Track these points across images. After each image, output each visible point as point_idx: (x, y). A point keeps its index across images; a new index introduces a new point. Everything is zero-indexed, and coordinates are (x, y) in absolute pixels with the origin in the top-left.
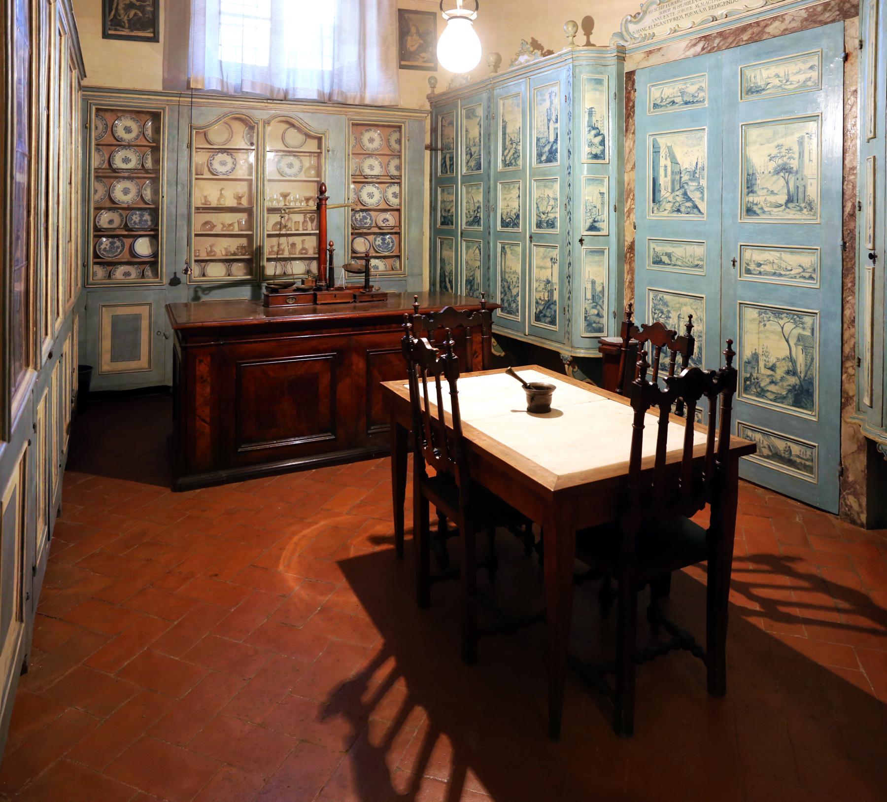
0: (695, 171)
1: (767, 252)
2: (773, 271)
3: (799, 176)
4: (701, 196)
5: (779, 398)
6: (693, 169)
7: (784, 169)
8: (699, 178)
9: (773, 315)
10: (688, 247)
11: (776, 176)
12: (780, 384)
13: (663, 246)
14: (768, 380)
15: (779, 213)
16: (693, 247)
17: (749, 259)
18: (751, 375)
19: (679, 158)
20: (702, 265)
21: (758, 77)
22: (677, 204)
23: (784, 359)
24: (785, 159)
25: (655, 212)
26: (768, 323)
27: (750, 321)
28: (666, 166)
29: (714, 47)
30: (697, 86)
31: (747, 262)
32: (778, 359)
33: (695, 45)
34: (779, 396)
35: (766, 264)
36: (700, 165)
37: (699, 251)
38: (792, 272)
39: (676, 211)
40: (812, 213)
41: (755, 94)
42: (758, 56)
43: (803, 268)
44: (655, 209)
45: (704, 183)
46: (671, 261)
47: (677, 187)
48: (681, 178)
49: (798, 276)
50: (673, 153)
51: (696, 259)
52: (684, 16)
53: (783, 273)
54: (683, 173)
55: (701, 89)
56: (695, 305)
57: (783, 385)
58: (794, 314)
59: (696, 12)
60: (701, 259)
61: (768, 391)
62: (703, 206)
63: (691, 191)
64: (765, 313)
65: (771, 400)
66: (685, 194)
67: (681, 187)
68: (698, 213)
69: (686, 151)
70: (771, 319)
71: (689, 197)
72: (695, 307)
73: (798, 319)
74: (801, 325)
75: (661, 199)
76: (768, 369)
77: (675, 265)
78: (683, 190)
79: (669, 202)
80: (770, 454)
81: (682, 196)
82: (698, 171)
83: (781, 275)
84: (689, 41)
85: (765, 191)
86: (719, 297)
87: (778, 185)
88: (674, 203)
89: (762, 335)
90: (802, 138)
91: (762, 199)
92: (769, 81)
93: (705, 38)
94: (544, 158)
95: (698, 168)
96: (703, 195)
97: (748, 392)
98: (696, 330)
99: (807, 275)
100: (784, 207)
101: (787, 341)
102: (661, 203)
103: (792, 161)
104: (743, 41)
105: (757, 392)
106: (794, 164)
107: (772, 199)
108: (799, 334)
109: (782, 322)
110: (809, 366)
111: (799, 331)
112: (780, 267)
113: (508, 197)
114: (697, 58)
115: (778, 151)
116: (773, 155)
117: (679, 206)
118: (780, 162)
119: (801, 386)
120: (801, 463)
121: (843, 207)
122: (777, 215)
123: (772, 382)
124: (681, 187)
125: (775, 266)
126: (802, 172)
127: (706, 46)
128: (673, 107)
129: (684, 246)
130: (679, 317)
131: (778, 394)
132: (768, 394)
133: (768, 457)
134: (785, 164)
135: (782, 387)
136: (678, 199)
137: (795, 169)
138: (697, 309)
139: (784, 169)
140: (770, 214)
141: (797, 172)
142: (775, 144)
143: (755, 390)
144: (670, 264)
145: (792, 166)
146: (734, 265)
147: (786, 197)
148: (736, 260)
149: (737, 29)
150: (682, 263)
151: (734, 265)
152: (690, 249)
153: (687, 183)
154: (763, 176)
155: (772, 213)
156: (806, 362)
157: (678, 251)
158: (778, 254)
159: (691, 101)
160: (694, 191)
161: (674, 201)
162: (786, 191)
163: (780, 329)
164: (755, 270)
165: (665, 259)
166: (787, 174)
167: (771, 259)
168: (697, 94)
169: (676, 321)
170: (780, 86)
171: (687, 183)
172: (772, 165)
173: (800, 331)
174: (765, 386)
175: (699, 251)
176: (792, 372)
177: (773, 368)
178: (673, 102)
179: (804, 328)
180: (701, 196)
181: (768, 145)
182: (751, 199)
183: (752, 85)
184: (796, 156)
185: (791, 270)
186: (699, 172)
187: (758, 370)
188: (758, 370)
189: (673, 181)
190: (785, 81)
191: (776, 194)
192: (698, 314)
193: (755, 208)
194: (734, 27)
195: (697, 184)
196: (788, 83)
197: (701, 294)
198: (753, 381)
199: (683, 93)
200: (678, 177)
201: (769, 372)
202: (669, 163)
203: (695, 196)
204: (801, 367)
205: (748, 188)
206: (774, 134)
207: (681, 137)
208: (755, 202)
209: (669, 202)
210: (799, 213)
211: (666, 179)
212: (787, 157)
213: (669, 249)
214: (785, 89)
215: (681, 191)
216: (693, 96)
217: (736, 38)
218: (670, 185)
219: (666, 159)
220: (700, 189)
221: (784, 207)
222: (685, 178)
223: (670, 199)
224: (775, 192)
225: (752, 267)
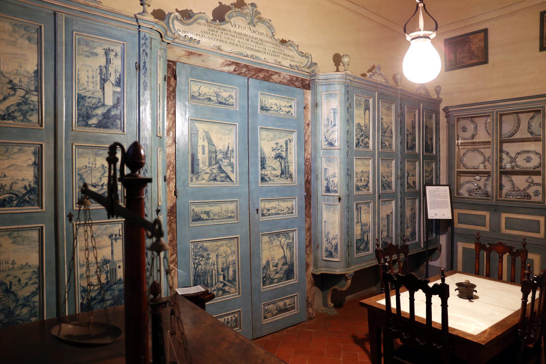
0: (227, 152)
1: (272, 202)
2: (276, 212)
3: (286, 161)
4: (232, 169)
5: (280, 280)
6: (226, 150)
7: (279, 156)
8: (230, 157)
9: (276, 236)
10: (223, 205)
12: (280, 272)
13: (202, 207)
14: (274, 273)
15: (278, 180)
16: (227, 204)
17: (263, 207)
18: (266, 274)
19: (214, 140)
20: (234, 216)
21: (267, 101)
22: (214, 175)
23: (281, 258)
24: (280, 151)
25: (194, 181)
26: (273, 242)
27: (265, 243)
28: (203, 146)
29: (242, 73)
30: (228, 94)
31: (262, 209)
32: (279, 259)
33: (229, 65)
34: (280, 279)
35: (272, 209)
36: (230, 149)
37: (232, 207)
38: (284, 211)
39: (213, 180)
40: (292, 180)
41: (265, 111)
42: (269, 90)
43: (288, 208)
44: (194, 178)
46: (209, 217)
47: (214, 162)
48: (216, 156)
49: (287, 213)
50: (210, 137)
51: (229, 212)
52: (228, 43)
53: (280, 212)
54: (218, 152)
55: (231, 96)
56: (229, 244)
57: (281, 272)
58: (285, 233)
59: (237, 45)
60: (233, 212)
61: (275, 279)
62: (233, 177)
63: (224, 166)
64: (272, 236)
65: (276, 283)
66: (220, 168)
67: (217, 163)
68: (229, 181)
69: (220, 137)
70: (275, 239)
71: (223, 170)
72: (229, 245)
74: (288, 238)
75: (200, 171)
76: (274, 267)
77: (213, 219)
78: (218, 165)
79: (207, 173)
80: (277, 312)
81: (218, 169)
82: (229, 152)
83: (279, 214)
84: (224, 61)
86: (249, 234)
87: (276, 164)
88: (211, 174)
89: (271, 249)
90: (287, 141)
91: (269, 172)
92: (272, 106)
93: (237, 64)
95: (229, 150)
96: (233, 169)
97: (265, 284)
98: (231, 261)
99: (290, 212)
100: (279, 177)
101: (283, 248)
102: (200, 174)
103: (283, 153)
104: (260, 77)
105: (270, 282)
106: (284, 154)
107: (274, 172)
108: (288, 243)
109: (280, 239)
110: (292, 257)
111: (288, 241)
112: (278, 210)
114: (231, 75)
115: (276, 146)
117: (216, 176)
118: (277, 152)
119: (289, 268)
120: (290, 307)
121: (305, 176)
122: (277, 181)
123: (277, 273)
124: (217, 163)
125: (276, 210)
127: (237, 69)
128: (210, 103)
129: (220, 205)
130: (217, 256)
131: (279, 278)
132: (276, 281)
133: (276, 314)
134: (280, 154)
135: (281, 273)
136: (215, 171)
137: (284, 157)
138: (231, 246)
140: (274, 181)
141: (285, 158)
142: (275, 142)
143: (268, 282)
144: (208, 220)
145: (283, 155)
146: (257, 212)
147: (280, 172)
148: (258, 209)
149: (257, 68)
150: (219, 217)
151: (257, 212)
152: (224, 207)
153: (221, 160)
154: (269, 159)
155: (274, 180)
156: (291, 256)
157: (215, 209)
158: (277, 203)
159: (224, 102)
160: (227, 165)
161: (211, 173)
162: (280, 168)
163: (279, 243)
164: (266, 213)
165: (204, 216)
166: (281, 159)
167: (274, 206)
168: (228, 99)
169: (215, 259)
170: (277, 111)
171: (221, 160)
172: (273, 154)
173: (288, 241)
174: (273, 277)
175: (232, 207)
176: (285, 264)
177: (276, 266)
178: (210, 99)
179: (289, 239)
180: (232, 169)
181: (271, 142)
182: (263, 172)
183: (264, 105)
184: (284, 150)
185: (284, 210)
186: (230, 153)
187: (269, 270)
188: (269, 270)
189: (210, 158)
190: (279, 109)
191: (276, 170)
192: (232, 249)
193: (266, 178)
195: (228, 161)
196: (281, 110)
197: (236, 235)
198: (267, 277)
199: (217, 95)
200: (214, 155)
201: (275, 268)
202: (206, 144)
203: (228, 170)
204: (288, 260)
205: (261, 165)
206: (274, 136)
207: (216, 127)
208: (266, 174)
209: (207, 173)
210: (286, 180)
211: (203, 155)
212: (280, 150)
213: (207, 208)
214: (279, 113)
215: (217, 166)
216: (225, 99)
217: (255, 74)
218: (207, 160)
219: (204, 140)
220: (231, 165)
221: (279, 177)
222: (220, 156)
223: (208, 171)
224: (275, 169)
225: (265, 212)
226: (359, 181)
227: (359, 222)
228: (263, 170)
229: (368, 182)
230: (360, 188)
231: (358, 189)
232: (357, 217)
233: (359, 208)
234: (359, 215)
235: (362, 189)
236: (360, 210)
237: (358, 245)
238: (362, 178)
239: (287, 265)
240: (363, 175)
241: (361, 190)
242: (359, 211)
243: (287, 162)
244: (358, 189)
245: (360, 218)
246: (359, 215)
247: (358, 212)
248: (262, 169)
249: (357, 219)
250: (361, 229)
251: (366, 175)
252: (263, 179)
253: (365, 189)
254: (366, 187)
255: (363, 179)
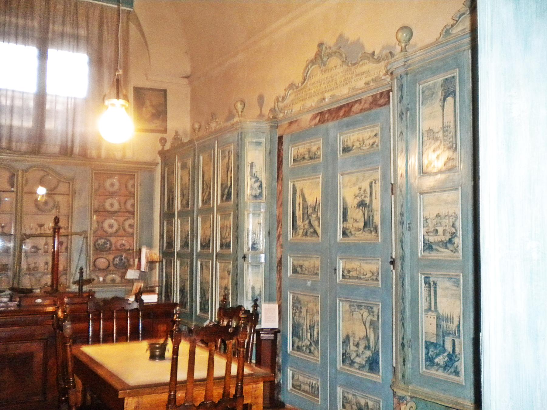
11: (358, 209)
24: (363, 197)
26: (354, 313)
40: (377, 235)
45: (320, 214)
48: (308, 212)
49: (370, 279)
73: (370, 309)
83: (360, 278)
85: (353, 219)
94: (225, 198)
100: (362, 231)
106: (367, 201)
107: (356, 225)
109: (362, 312)
113: (205, 227)
116: (356, 195)
118: (360, 199)
126: (372, 206)
134: (363, 201)
137: (368, 204)
139: (362, 204)
145: (366, 202)
147: (363, 224)
164: (347, 275)
167: (355, 267)
172: (356, 202)
184: (368, 195)
194: (335, 106)
200: (306, 212)
221: (362, 231)
226: (432, 234)
227: (433, 309)
228: (345, 223)
229: (454, 235)
230: (434, 247)
231: (429, 247)
232: (428, 299)
233: (432, 284)
234: (433, 297)
235: (438, 248)
236: (435, 288)
237: (431, 353)
238: (436, 228)
239: (370, 352)
240: (440, 223)
241: (437, 250)
242: (432, 288)
243: (372, 211)
244: (429, 247)
245: (436, 303)
246: (433, 297)
247: (430, 291)
248: (343, 221)
249: (427, 304)
250: (437, 325)
251: (447, 221)
252: (344, 234)
253: (447, 248)
254: (449, 245)
255: (440, 230)
